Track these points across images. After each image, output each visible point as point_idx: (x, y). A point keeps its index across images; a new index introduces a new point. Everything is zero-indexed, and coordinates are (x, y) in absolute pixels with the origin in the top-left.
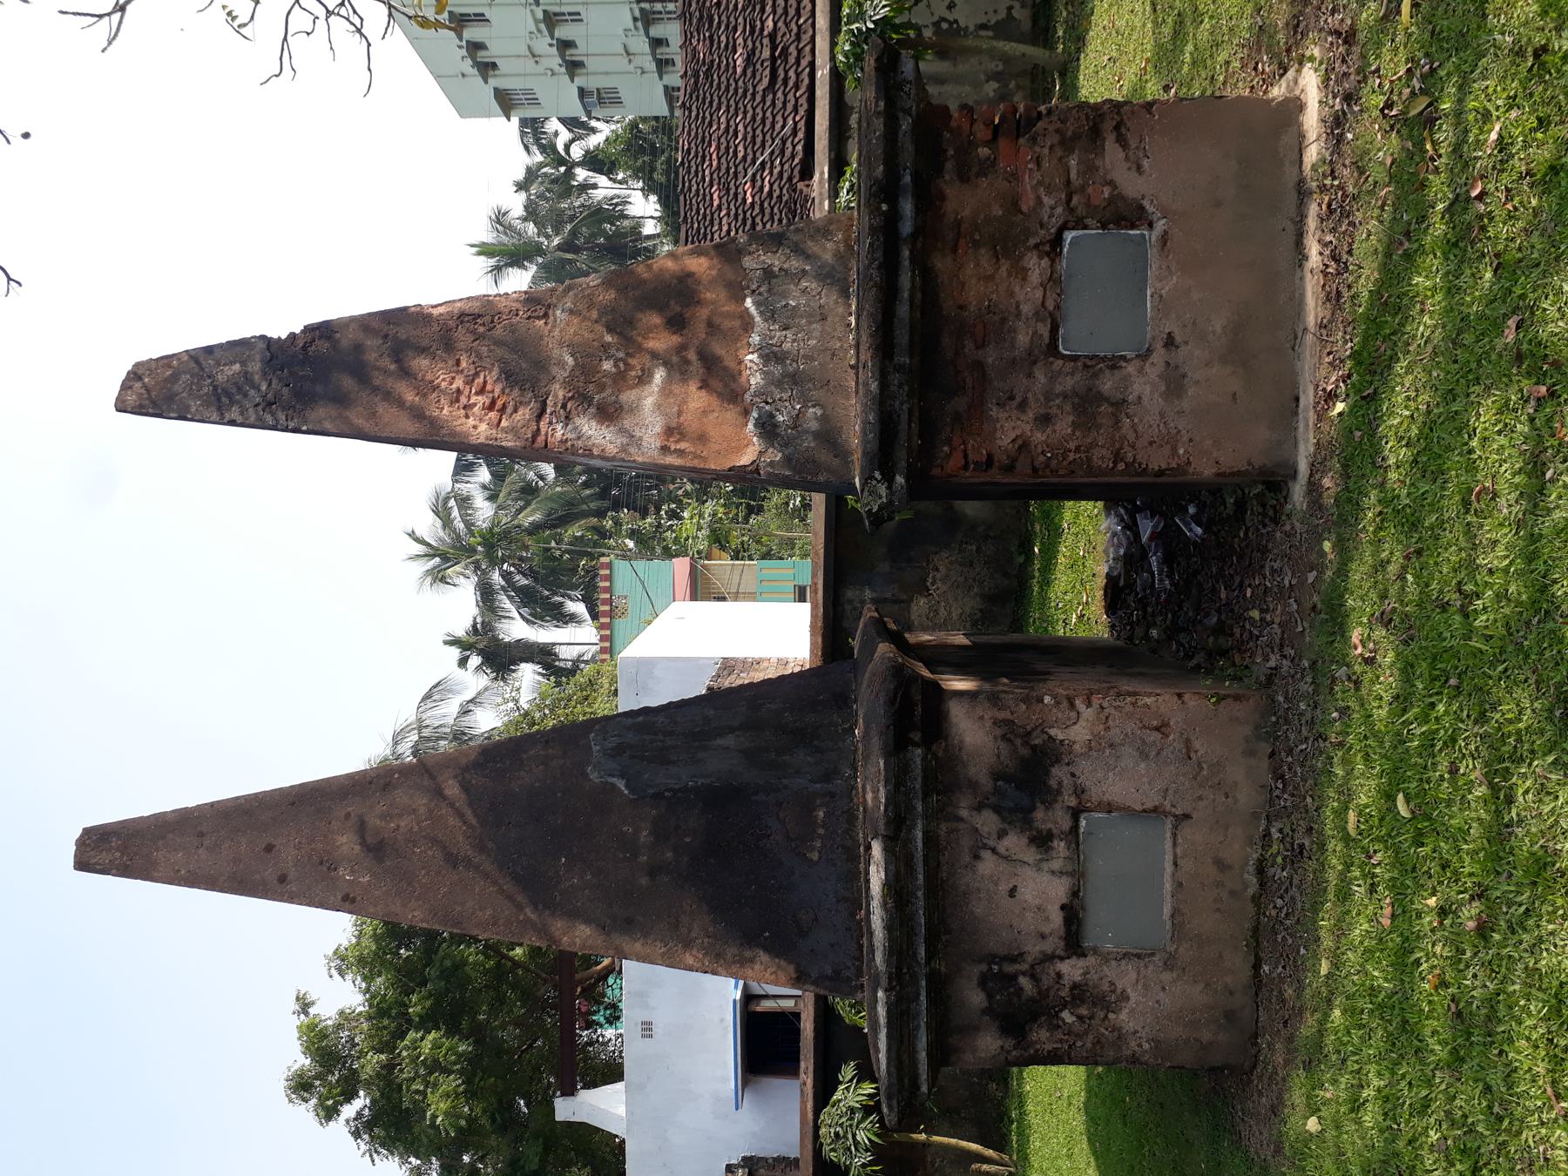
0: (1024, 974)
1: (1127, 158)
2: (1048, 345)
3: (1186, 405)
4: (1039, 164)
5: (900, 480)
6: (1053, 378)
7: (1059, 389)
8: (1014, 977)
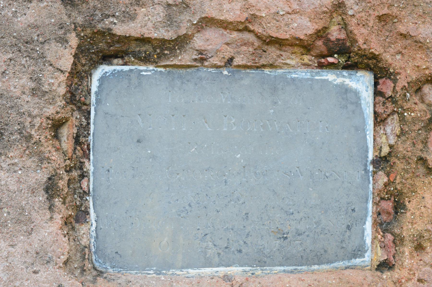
2: (107, 33)
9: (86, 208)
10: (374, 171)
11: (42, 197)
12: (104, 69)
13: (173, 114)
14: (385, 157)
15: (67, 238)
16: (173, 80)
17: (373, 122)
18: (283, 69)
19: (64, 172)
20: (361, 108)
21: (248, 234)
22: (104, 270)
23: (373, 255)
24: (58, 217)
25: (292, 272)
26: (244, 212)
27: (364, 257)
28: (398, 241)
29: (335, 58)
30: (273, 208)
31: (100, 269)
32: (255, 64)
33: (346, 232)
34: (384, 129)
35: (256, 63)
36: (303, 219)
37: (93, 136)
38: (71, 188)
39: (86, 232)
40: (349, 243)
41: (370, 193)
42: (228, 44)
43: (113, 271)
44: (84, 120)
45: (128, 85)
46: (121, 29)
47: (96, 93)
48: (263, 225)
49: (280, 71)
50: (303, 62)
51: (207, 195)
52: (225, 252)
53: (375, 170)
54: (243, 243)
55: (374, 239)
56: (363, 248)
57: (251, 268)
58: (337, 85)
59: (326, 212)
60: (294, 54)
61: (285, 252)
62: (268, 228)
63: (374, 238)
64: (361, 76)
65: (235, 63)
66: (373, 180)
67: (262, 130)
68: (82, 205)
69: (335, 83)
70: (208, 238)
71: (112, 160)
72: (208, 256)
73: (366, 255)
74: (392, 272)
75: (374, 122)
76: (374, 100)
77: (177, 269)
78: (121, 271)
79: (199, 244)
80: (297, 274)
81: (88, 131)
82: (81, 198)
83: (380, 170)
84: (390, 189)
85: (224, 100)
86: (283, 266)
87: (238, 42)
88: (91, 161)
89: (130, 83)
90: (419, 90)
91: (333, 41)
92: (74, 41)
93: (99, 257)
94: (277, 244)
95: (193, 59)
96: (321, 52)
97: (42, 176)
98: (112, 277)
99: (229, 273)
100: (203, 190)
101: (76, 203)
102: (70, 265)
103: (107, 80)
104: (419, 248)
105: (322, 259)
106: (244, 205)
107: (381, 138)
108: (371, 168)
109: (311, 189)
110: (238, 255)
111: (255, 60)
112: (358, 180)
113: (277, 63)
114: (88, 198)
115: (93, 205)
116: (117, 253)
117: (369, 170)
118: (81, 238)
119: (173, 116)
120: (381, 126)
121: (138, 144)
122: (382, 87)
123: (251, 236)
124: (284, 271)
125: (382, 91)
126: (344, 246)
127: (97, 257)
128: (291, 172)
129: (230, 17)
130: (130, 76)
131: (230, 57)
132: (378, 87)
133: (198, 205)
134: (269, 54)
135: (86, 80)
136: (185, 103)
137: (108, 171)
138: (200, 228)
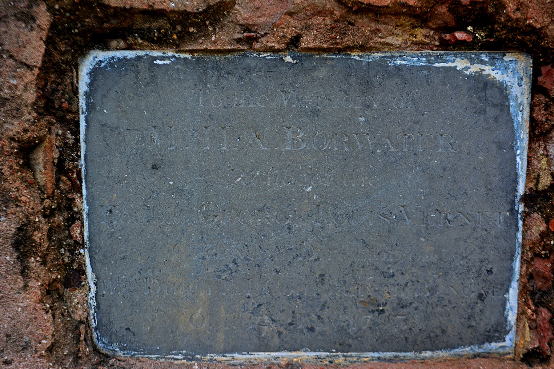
9: (79, 265)
10: (524, 212)
11: (10, 257)
12: (97, 56)
13: (206, 125)
14: (544, 191)
15: (50, 315)
16: (204, 72)
17: (528, 135)
18: (381, 52)
19: (42, 219)
20: (509, 113)
21: (323, 306)
22: (110, 353)
23: (519, 339)
24: (35, 285)
25: (390, 360)
26: (318, 273)
27: (504, 341)
29: (468, 32)
30: (363, 267)
31: (104, 351)
32: (335, 46)
33: (477, 303)
34: (545, 147)
35: (336, 43)
36: (410, 284)
37: (85, 160)
38: (54, 241)
39: (81, 301)
40: (481, 320)
41: (517, 245)
42: (291, 14)
43: (124, 354)
44: (70, 136)
45: (135, 80)
47: (86, 93)
48: (347, 291)
49: (377, 55)
50: (414, 39)
51: (260, 248)
52: (289, 330)
53: (527, 210)
54: (316, 317)
55: (522, 314)
56: (503, 327)
57: (328, 354)
58: (470, 77)
59: (446, 273)
60: (400, 28)
61: (380, 332)
62: (355, 296)
63: (521, 314)
64: (510, 60)
65: (303, 45)
66: (524, 225)
67: (347, 149)
68: (73, 261)
69: (468, 73)
70: (262, 310)
71: (115, 195)
72: (263, 335)
73: (507, 338)
74: (545, 366)
75: (530, 134)
76: (532, 99)
77: (217, 353)
78: (135, 354)
79: (250, 318)
80: (399, 363)
81: (78, 152)
82: (72, 252)
83: (534, 211)
84: (548, 242)
85: (286, 103)
86: (377, 351)
87: (308, 10)
88: (84, 197)
89: (137, 78)
91: (465, 5)
92: (44, 18)
93: (102, 335)
94: (368, 320)
95: (235, 40)
96: (445, 22)
98: (122, 363)
99: (295, 360)
100: (255, 241)
101: (63, 261)
102: (57, 351)
103: (103, 74)
105: (437, 342)
106: (317, 263)
107: (539, 162)
108: (521, 208)
109: (423, 240)
110: (309, 335)
111: (335, 38)
112: (499, 226)
113: (371, 44)
114: (82, 251)
115: (90, 261)
116: (128, 329)
117: (518, 211)
118: (74, 310)
119: (206, 128)
120: (541, 143)
121: (153, 171)
122: (544, 80)
123: (328, 308)
124: (379, 358)
125: (545, 86)
126: (473, 323)
127: (99, 334)
128: (391, 213)
130: (137, 67)
131: (295, 35)
132: (540, 79)
133: (247, 262)
134: (359, 29)
135: (70, 74)
136: (225, 107)
137: (111, 211)
138: (251, 296)
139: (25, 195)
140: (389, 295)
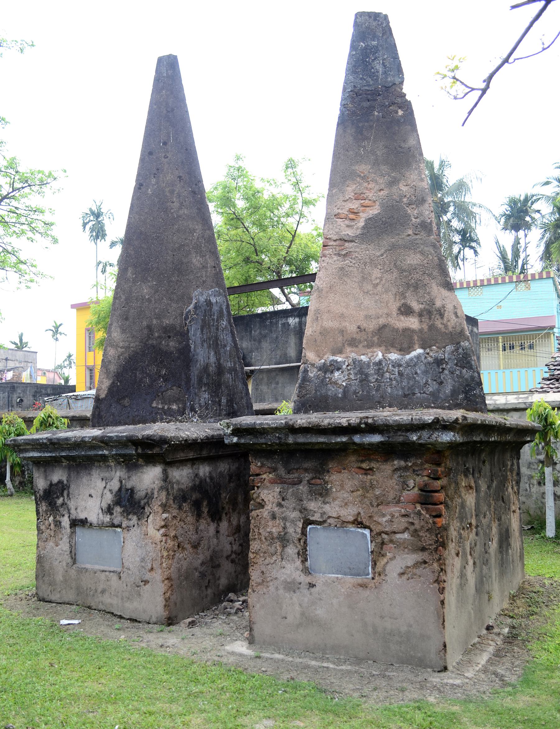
0: (64, 500)
1: (408, 567)
2: (309, 519)
3: (281, 591)
4: (404, 516)
5: (235, 440)
6: (293, 522)
7: (288, 524)
8: (63, 496)
11: (297, 556)
12: (310, 526)
28: (375, 573)
46: (311, 519)
90: (380, 534)
92: (302, 521)
97: (296, 551)
104: (380, 575)
129: (334, 516)
139: (299, 546)
140: (352, 567)
